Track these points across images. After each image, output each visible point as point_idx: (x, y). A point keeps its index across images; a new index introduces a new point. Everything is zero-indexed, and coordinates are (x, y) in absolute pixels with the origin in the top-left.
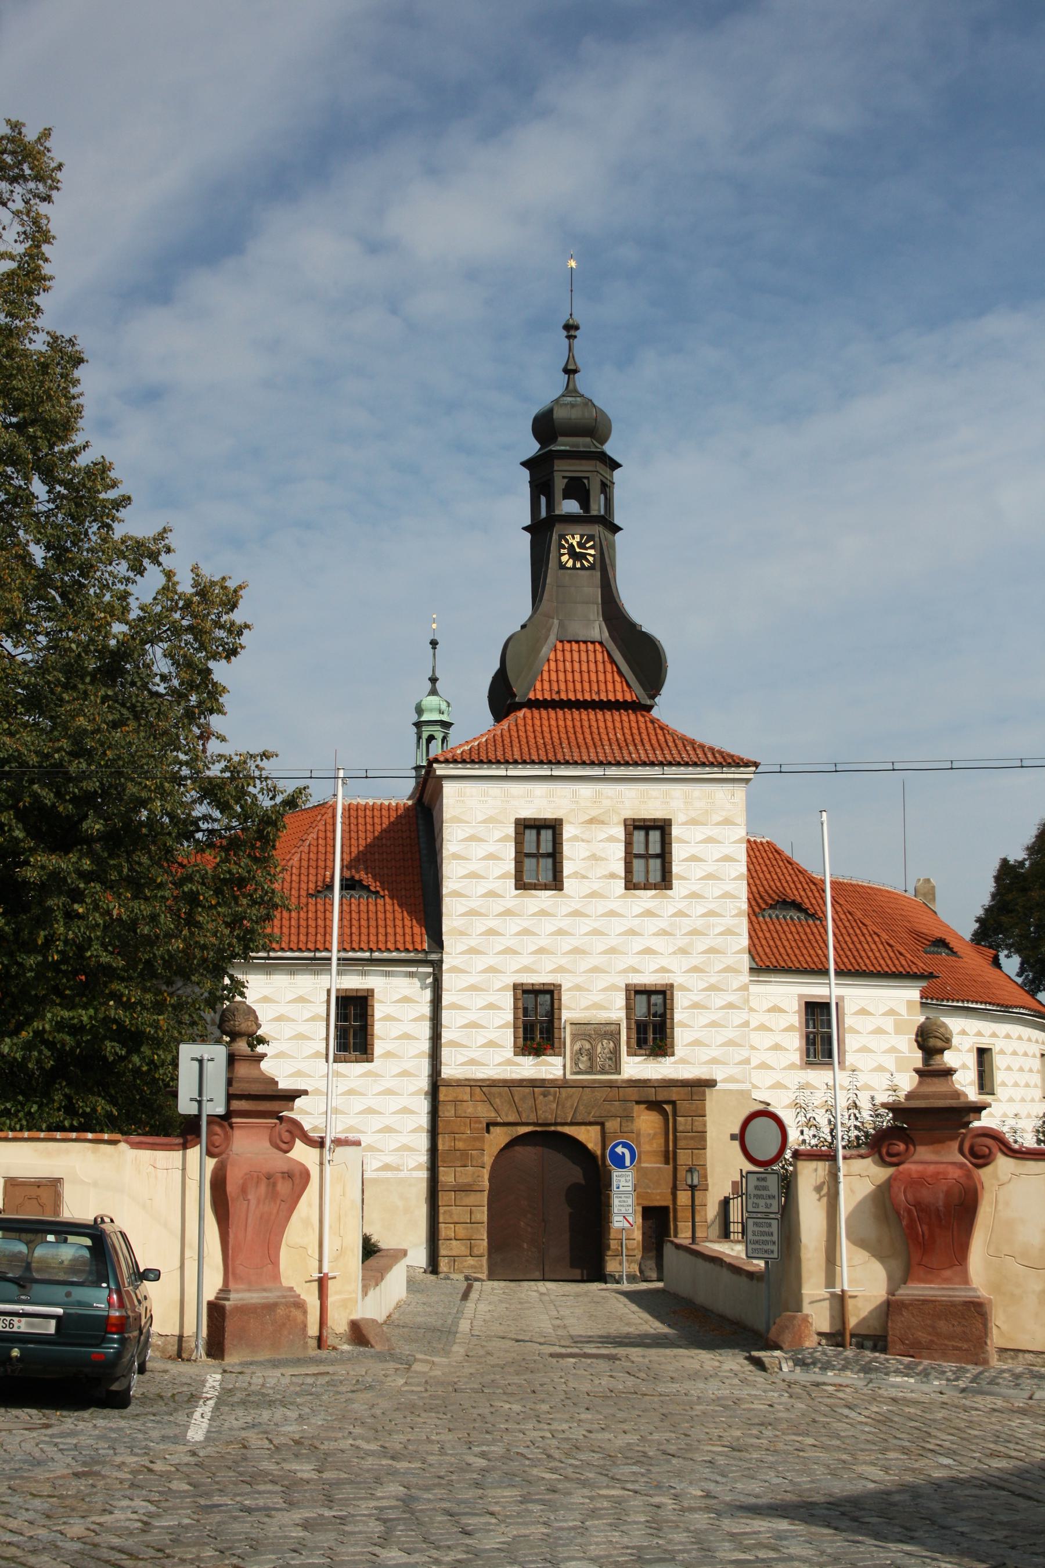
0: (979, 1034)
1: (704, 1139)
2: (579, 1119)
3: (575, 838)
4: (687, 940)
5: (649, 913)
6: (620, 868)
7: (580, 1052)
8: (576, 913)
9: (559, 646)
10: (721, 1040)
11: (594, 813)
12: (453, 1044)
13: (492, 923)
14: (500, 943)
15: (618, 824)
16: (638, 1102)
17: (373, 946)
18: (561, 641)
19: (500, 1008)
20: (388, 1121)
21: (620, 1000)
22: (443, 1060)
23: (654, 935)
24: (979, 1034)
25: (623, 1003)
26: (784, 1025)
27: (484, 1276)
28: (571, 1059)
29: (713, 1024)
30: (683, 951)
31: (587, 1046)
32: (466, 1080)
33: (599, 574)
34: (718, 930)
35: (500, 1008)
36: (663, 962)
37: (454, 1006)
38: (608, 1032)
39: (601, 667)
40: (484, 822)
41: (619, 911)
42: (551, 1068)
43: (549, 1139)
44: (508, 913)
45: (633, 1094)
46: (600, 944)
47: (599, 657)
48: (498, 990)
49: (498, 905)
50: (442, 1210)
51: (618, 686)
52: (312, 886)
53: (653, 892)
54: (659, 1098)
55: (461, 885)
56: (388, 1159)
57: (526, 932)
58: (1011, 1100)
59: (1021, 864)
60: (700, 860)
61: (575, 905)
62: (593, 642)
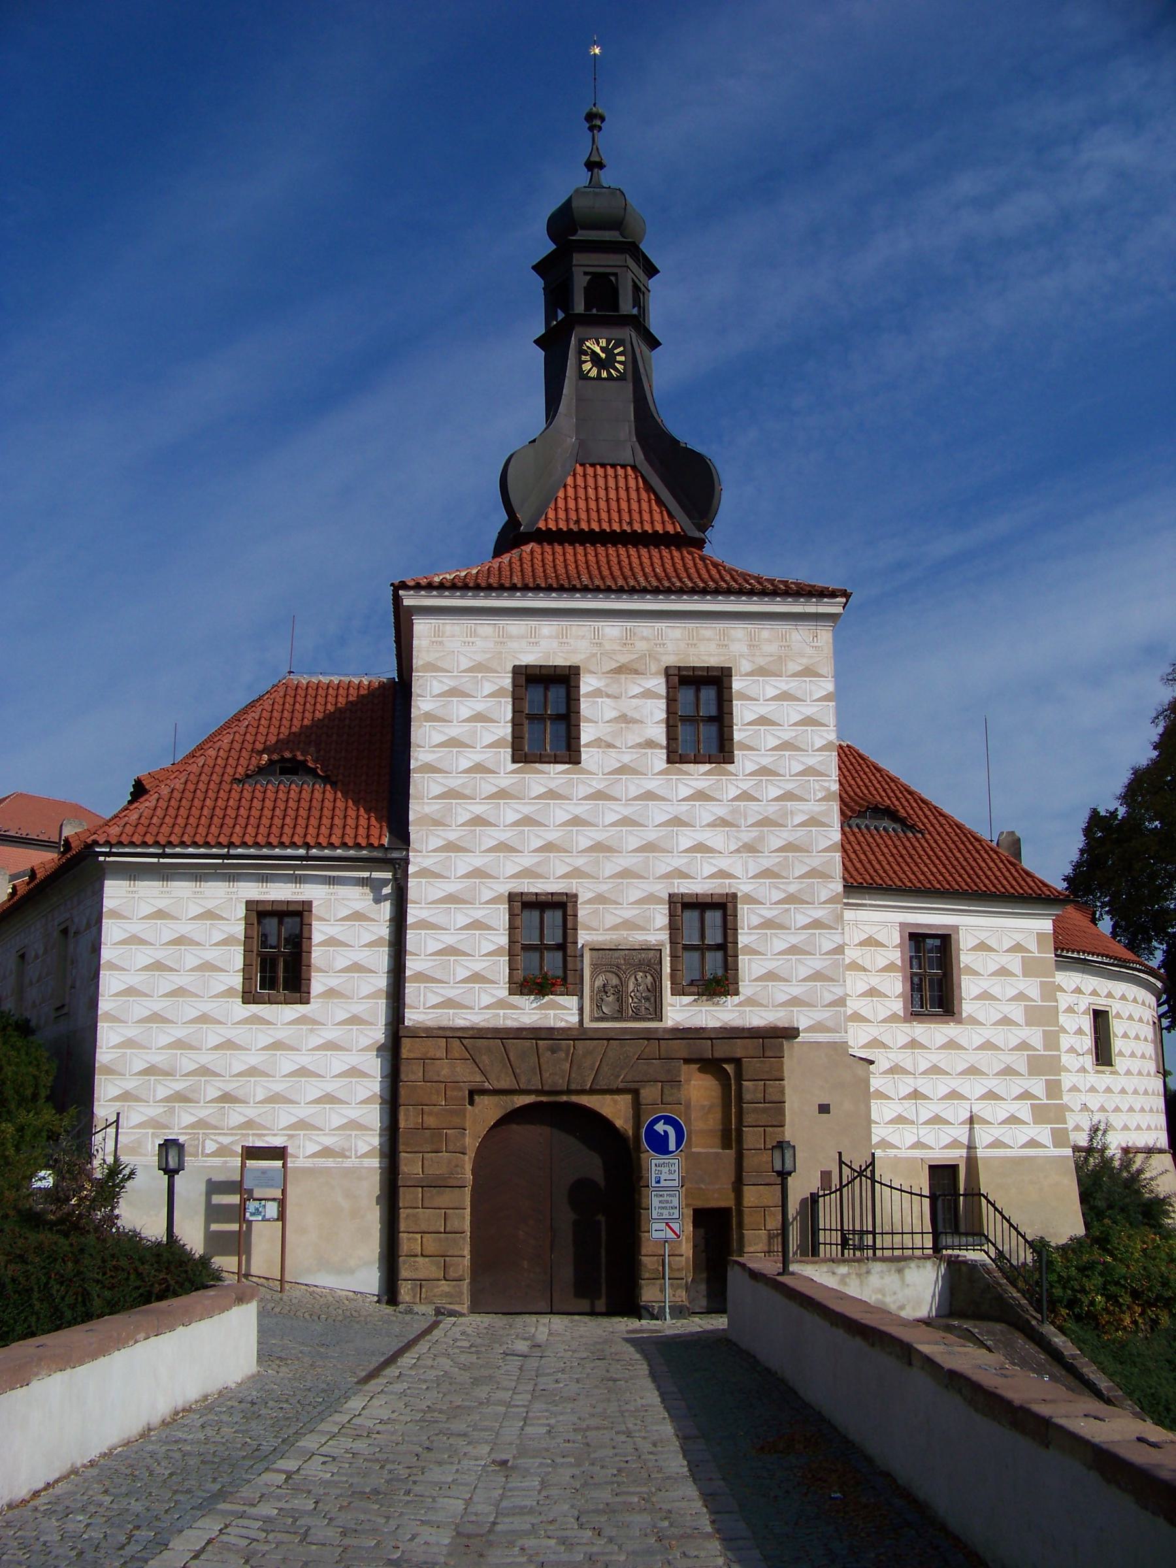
0: (1094, 993)
1: (781, 1112)
2: (602, 1084)
3: (597, 693)
4: (754, 833)
5: (701, 796)
6: (659, 733)
7: (604, 989)
8: (599, 796)
9: (579, 469)
10: (804, 972)
11: (623, 659)
12: (421, 977)
13: (479, 809)
14: (491, 837)
15: (656, 674)
16: (687, 1061)
17: (310, 840)
18: (582, 465)
19: (489, 928)
20: (330, 1087)
21: (661, 917)
22: (408, 1000)
23: (708, 825)
24: (1094, 993)
25: (666, 921)
26: (882, 963)
27: (464, 1309)
28: (592, 999)
29: (793, 950)
30: (750, 848)
31: (615, 981)
32: (440, 1028)
33: (631, 385)
34: (798, 819)
35: (489, 928)
36: (723, 863)
37: (424, 925)
38: (644, 961)
39: (634, 495)
40: (469, 670)
41: (660, 792)
42: (562, 1011)
43: (561, 1115)
44: (502, 794)
45: (680, 1048)
46: (633, 839)
47: (632, 483)
48: (487, 903)
49: (488, 786)
50: (403, 1213)
51: (657, 517)
52: (240, 770)
53: (707, 767)
54: (717, 1055)
55: (435, 756)
56: (328, 1141)
57: (527, 821)
58: (1128, 1073)
59: (1113, 814)
60: (773, 723)
61: (598, 784)
62: (624, 467)
